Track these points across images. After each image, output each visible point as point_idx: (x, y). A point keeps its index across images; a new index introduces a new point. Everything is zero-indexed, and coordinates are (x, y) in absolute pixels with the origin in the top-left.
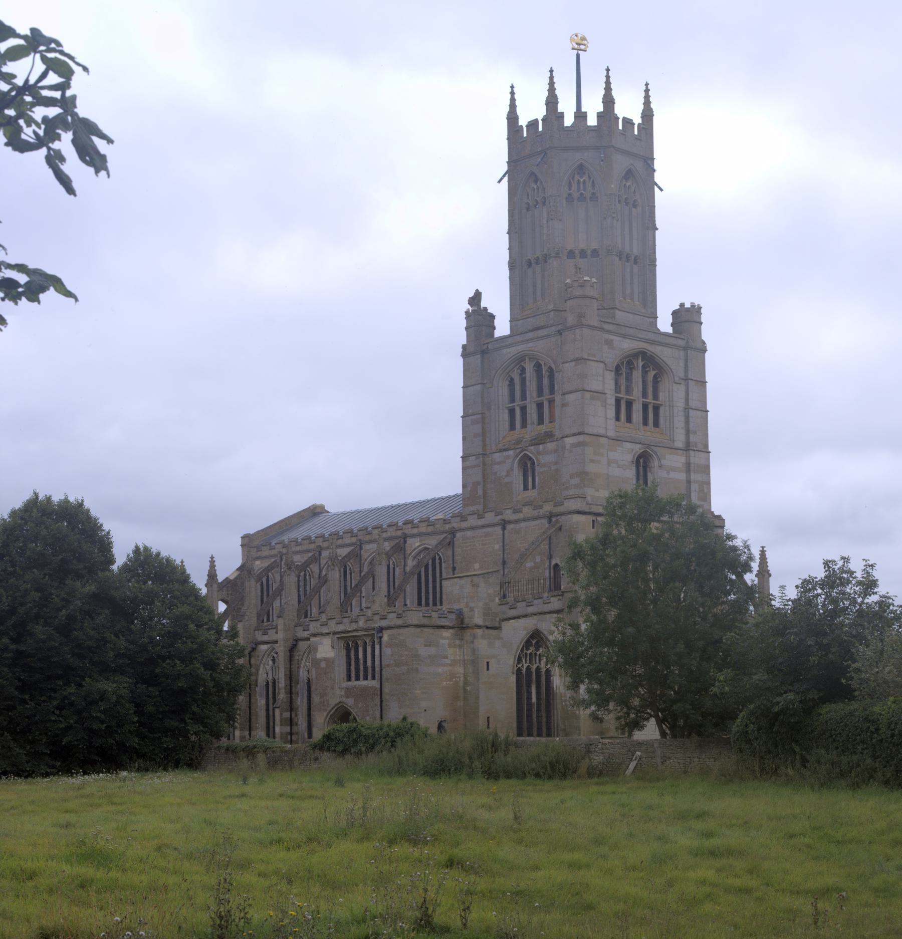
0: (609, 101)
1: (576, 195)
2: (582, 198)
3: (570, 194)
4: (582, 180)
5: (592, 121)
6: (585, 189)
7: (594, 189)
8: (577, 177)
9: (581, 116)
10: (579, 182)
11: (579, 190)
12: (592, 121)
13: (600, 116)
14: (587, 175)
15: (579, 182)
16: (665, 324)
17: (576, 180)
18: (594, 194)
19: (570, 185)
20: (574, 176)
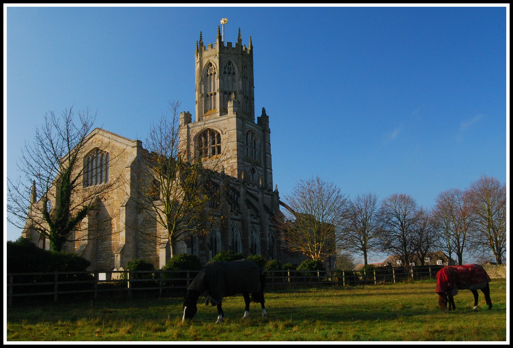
0: (240, 40)
1: (227, 72)
2: (229, 73)
3: (225, 71)
4: (230, 67)
5: (234, 46)
6: (230, 70)
7: (234, 70)
8: (228, 65)
9: (230, 44)
10: (228, 67)
11: (228, 70)
12: (234, 46)
13: (236, 44)
14: (231, 65)
15: (228, 67)
16: (256, 122)
17: (227, 66)
18: (234, 72)
19: (225, 68)
20: (226, 65)
